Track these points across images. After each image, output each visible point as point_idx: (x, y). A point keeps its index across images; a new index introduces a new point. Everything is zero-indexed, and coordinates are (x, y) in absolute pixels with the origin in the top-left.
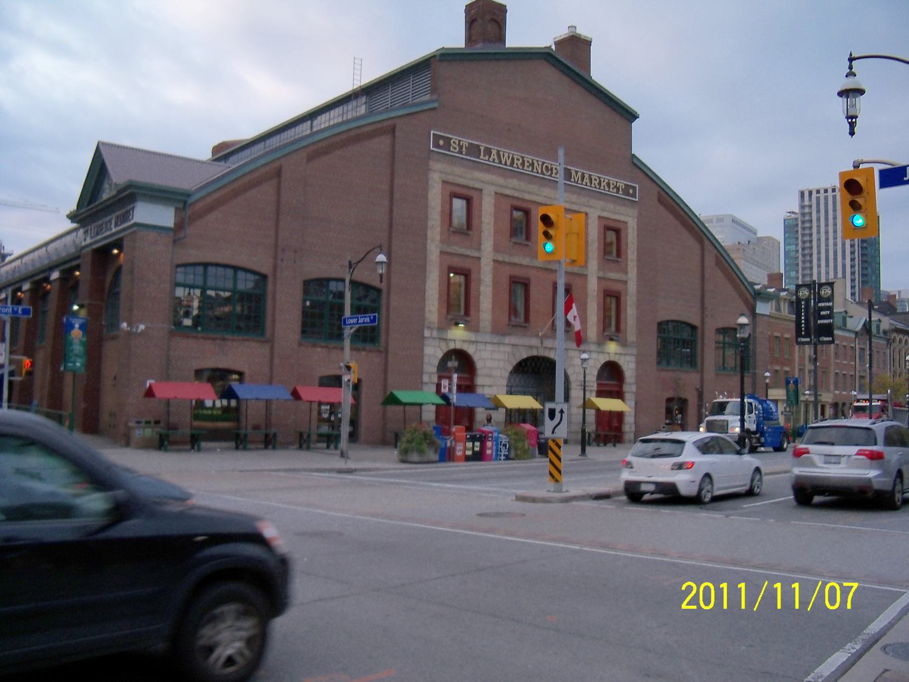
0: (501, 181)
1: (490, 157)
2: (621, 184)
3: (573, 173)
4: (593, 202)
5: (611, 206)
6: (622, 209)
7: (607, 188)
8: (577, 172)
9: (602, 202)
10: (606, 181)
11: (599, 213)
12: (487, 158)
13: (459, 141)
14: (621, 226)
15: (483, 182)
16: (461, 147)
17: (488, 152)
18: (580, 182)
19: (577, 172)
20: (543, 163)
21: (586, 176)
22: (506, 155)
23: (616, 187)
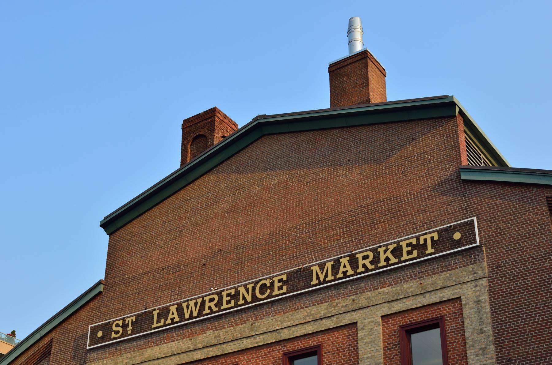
0: (186, 344)
1: (166, 320)
2: (430, 236)
3: (315, 269)
4: (362, 300)
5: (411, 286)
6: (440, 279)
7: (393, 260)
8: (322, 266)
9: (387, 290)
10: (391, 247)
11: (386, 310)
12: (162, 323)
13: (124, 319)
14: (444, 310)
15: (158, 359)
16: (125, 326)
17: (164, 313)
18: (330, 277)
19: (322, 266)
20: (256, 283)
21: (345, 261)
22: (192, 303)
23: (414, 247)
